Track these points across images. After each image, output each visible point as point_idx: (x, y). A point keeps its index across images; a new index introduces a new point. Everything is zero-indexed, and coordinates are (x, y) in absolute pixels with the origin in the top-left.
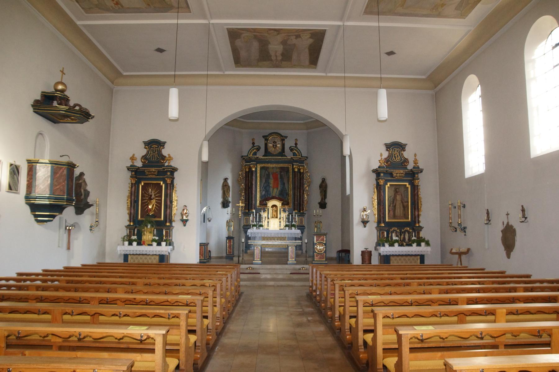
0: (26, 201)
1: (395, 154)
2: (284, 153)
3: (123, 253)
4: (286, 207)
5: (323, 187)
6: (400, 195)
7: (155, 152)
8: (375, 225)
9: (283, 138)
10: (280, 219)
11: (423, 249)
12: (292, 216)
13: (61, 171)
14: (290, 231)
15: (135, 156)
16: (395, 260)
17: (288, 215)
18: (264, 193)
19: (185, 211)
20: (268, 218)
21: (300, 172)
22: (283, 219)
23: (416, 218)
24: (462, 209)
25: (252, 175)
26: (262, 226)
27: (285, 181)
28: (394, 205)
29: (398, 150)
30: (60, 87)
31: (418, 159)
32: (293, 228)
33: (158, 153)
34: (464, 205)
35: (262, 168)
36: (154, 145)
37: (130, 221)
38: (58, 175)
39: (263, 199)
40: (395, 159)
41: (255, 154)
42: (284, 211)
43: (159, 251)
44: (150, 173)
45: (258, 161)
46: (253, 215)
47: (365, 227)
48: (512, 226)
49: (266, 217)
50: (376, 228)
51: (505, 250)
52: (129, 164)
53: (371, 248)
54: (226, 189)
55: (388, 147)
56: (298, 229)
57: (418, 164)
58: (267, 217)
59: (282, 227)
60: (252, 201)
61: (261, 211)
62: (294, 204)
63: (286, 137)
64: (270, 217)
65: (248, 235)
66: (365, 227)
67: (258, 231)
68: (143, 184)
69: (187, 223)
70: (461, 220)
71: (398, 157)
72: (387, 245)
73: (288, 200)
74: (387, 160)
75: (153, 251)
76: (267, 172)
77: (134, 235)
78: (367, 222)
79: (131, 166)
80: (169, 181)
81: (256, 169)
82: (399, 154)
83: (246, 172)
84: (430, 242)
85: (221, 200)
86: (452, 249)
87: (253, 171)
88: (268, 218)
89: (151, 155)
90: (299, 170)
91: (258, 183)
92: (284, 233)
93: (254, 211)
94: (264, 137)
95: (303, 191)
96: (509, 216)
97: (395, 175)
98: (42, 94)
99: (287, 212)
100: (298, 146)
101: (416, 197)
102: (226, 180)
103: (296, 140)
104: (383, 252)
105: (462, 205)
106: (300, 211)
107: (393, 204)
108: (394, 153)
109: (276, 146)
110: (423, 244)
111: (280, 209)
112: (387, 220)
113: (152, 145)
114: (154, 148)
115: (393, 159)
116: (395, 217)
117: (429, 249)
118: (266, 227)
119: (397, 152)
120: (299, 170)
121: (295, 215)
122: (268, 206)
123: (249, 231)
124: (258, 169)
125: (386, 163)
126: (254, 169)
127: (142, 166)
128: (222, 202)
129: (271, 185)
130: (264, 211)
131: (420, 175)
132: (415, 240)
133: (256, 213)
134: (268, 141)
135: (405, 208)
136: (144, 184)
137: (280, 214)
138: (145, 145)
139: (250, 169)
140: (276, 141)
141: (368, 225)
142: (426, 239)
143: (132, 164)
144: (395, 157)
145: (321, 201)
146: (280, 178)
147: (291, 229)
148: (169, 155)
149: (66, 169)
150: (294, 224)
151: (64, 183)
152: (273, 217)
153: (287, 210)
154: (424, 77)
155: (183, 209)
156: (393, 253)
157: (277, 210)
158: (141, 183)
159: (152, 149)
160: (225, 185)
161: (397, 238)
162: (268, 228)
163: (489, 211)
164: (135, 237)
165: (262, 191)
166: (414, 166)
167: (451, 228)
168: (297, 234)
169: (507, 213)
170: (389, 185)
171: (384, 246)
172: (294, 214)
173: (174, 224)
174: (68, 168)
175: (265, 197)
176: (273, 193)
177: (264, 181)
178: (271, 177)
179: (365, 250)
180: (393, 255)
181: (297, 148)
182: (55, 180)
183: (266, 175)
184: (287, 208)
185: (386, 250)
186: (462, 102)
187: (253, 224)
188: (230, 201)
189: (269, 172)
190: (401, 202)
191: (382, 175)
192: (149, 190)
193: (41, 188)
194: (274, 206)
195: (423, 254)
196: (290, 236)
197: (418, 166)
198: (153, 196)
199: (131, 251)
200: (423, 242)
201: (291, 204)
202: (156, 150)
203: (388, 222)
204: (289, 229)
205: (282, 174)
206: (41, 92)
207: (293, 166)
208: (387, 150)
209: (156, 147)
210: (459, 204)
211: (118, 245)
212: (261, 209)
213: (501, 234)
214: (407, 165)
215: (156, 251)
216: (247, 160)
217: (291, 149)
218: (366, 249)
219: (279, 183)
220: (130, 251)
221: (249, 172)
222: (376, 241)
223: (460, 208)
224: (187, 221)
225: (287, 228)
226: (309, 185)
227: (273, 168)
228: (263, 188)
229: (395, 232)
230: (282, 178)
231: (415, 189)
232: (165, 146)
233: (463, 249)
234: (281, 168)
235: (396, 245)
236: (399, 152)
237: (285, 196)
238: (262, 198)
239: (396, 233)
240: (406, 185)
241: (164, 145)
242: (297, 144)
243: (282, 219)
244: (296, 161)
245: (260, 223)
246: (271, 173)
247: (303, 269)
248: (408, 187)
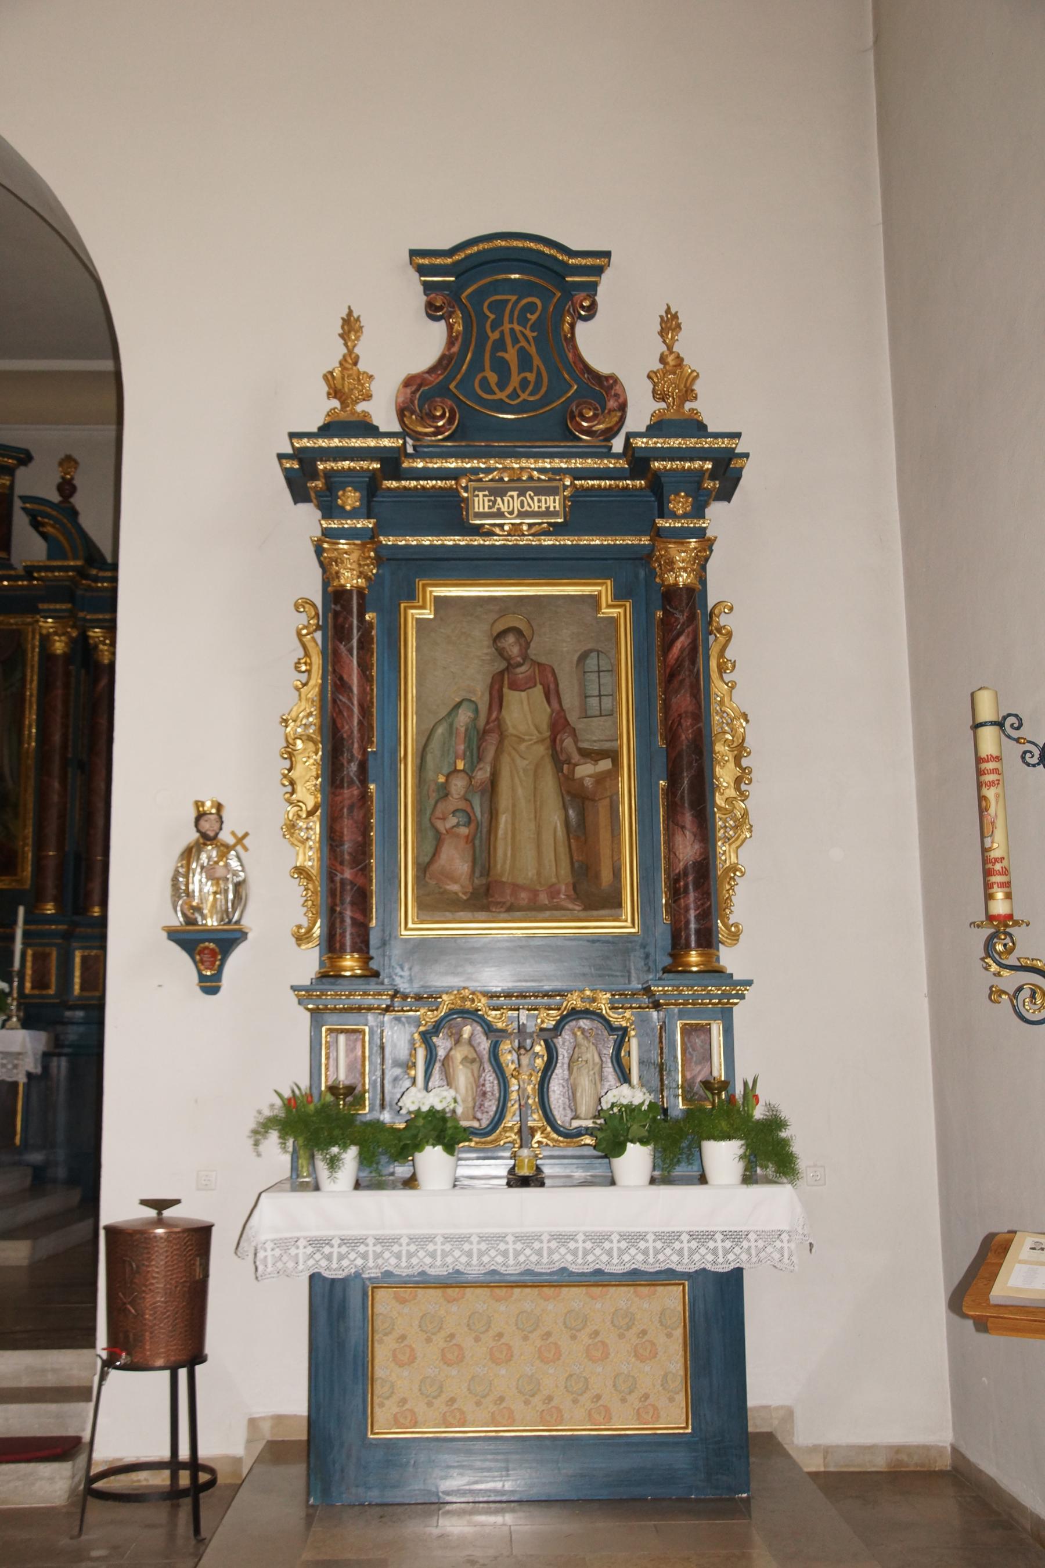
6: (538, 691)
28: (483, 774)
29: (531, 308)
108: (494, 336)
119: (523, 321)
144: (502, 368)
167: (1010, 980)
190: (541, 750)
195: (723, 1266)
218: (160, 1205)
240: (594, 601)
242: (73, 489)
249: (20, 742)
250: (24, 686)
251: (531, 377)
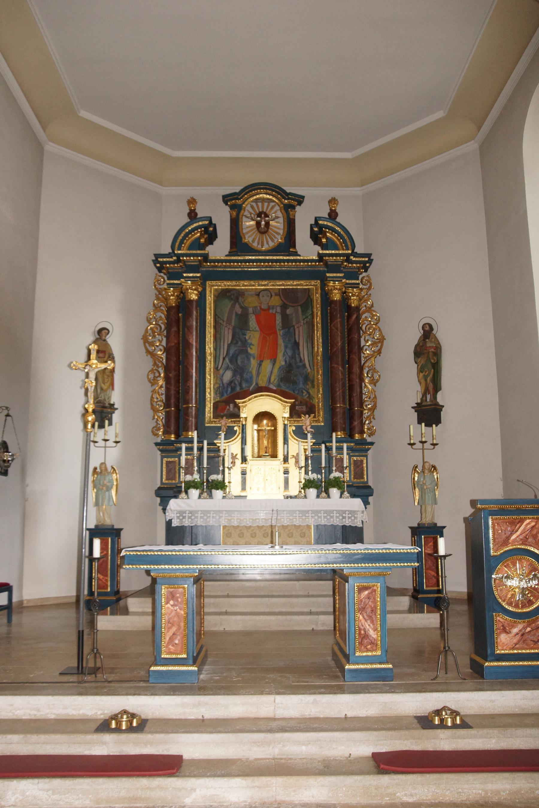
2: (294, 246)
4: (307, 421)
10: (286, 460)
12: (328, 449)
14: (324, 504)
17: (315, 450)
18: (228, 376)
20: (244, 460)
21: (349, 308)
22: (297, 462)
25: (188, 314)
32: (334, 492)
35: (221, 295)
39: (225, 396)
41: (197, 245)
42: (300, 433)
46: (189, 450)
49: (234, 457)
56: (353, 496)
58: (239, 456)
59: (295, 488)
60: (187, 401)
61: (217, 436)
62: (332, 412)
63: (300, 200)
64: (248, 453)
67: (206, 504)
76: (237, 306)
81: (202, 296)
83: (169, 309)
87: (191, 301)
88: (244, 460)
91: (210, 348)
92: (304, 513)
93: (195, 434)
94: (226, 199)
95: (361, 368)
99: (309, 436)
106: (351, 436)
109: (267, 224)
111: (285, 426)
118: (234, 488)
120: (345, 298)
121: (340, 449)
122: (243, 415)
123: (173, 503)
124: (210, 299)
126: (194, 297)
129: (253, 350)
130: (230, 434)
133: (200, 442)
134: (242, 211)
139: (182, 294)
145: (422, 399)
146: (283, 327)
147: (329, 497)
150: (336, 478)
152: (259, 457)
153: (309, 429)
157: (276, 429)
162: (243, 494)
165: (221, 371)
168: (351, 512)
172: (334, 444)
175: (233, 389)
176: (258, 374)
177: (228, 336)
178: (253, 322)
183: (234, 316)
184: (308, 423)
187: (189, 478)
189: (245, 309)
194: (260, 417)
196: (323, 522)
204: (318, 496)
205: (288, 311)
207: (323, 285)
212: (219, 429)
217: (316, 238)
219: (280, 341)
225: (312, 492)
226: (379, 352)
227: (258, 294)
228: (227, 360)
234: (285, 293)
237: (301, 385)
238: (222, 395)
243: (292, 461)
244: (336, 268)
245: (213, 477)
246: (251, 310)
249: (313, 348)
250: (313, 318)
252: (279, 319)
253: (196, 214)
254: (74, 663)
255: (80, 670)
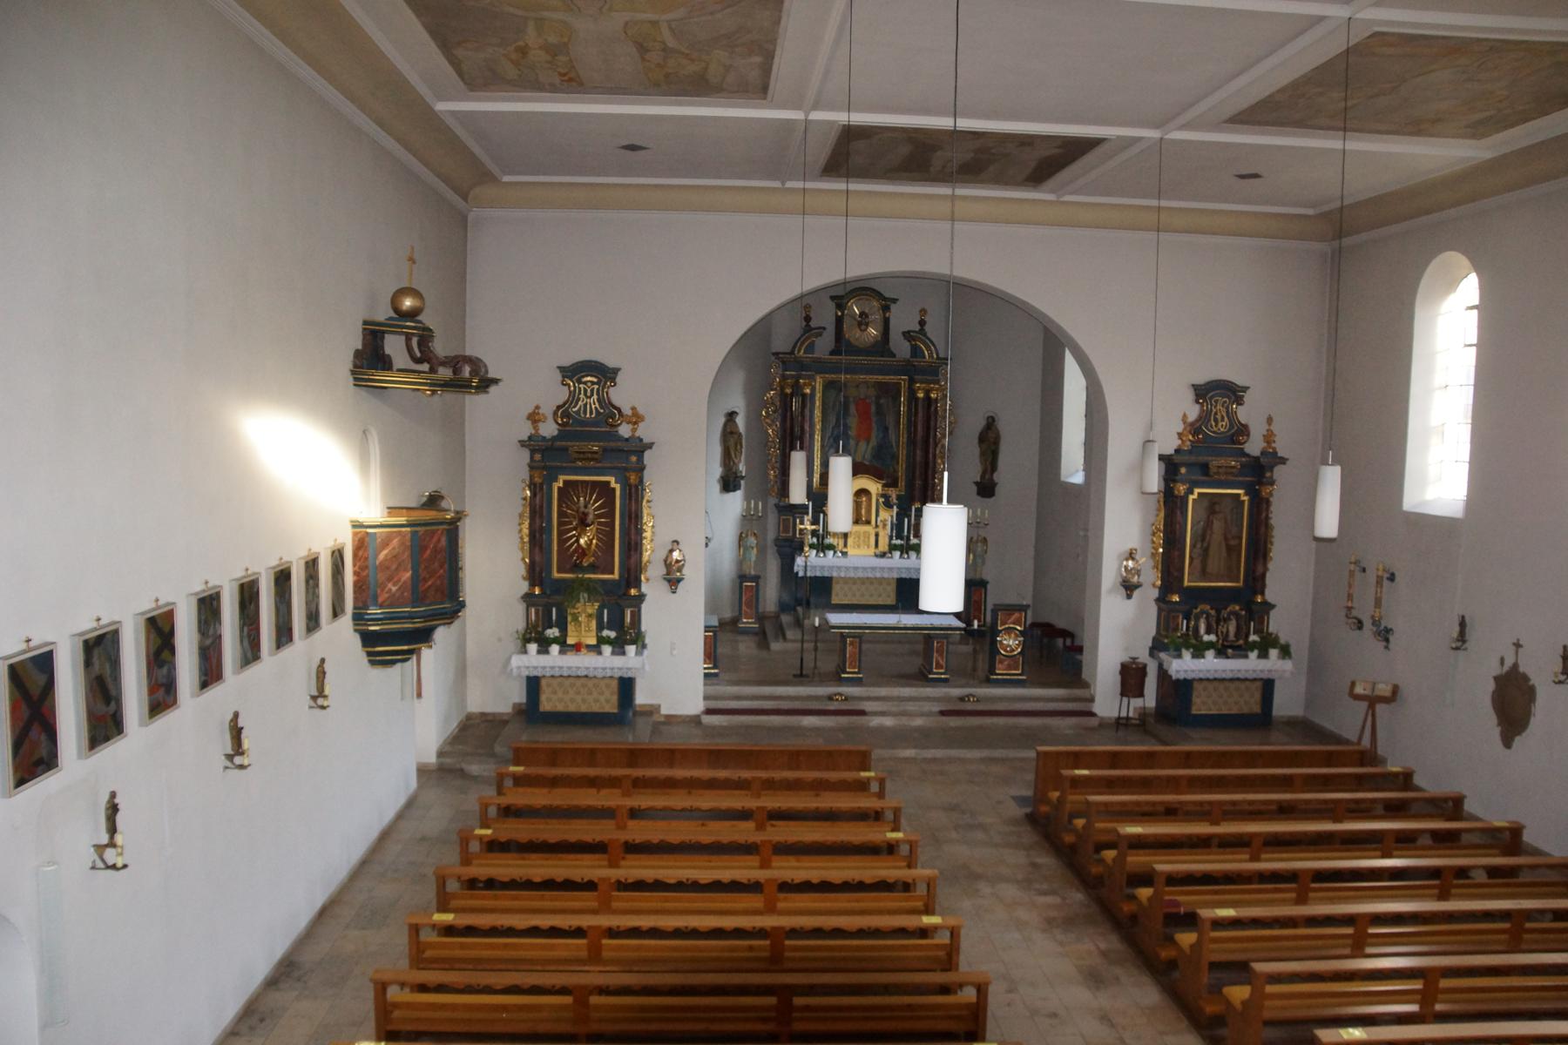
0: (355, 625)
1: (1216, 414)
3: (526, 673)
4: (893, 494)
5: (989, 440)
7: (592, 395)
8: (1155, 593)
9: (886, 304)
11: (1273, 664)
13: (435, 539)
15: (541, 411)
16: (1205, 689)
19: (676, 555)
23: (1256, 582)
24: (1386, 583)
26: (831, 547)
27: (890, 421)
28: (1205, 545)
29: (1225, 402)
30: (408, 303)
31: (1275, 432)
33: (598, 400)
34: (1393, 574)
35: (828, 386)
36: (587, 376)
37: (532, 585)
38: (428, 552)
40: (1216, 426)
42: (888, 505)
43: (620, 669)
44: (582, 456)
45: (820, 367)
47: (1129, 597)
48: (1525, 678)
50: (1158, 600)
51: (1499, 724)
52: (526, 430)
53: (1143, 656)
54: (731, 443)
55: (1203, 392)
57: (1273, 445)
63: (895, 301)
65: (797, 573)
66: (1129, 597)
68: (561, 485)
69: (681, 585)
70: (1380, 613)
71: (1223, 420)
72: (1187, 655)
73: (896, 471)
74: (1195, 428)
75: (604, 669)
77: (551, 627)
78: (1138, 586)
79: (530, 438)
80: (633, 478)
81: (813, 389)
82: (1227, 412)
84: (1292, 650)
85: (718, 471)
86: (1353, 684)
89: (580, 403)
90: (927, 392)
92: (891, 569)
96: (1520, 650)
97: (1213, 470)
98: (364, 329)
99: (895, 507)
100: (927, 328)
101: (1263, 529)
102: (731, 416)
103: (923, 311)
104: (1178, 672)
105: (1386, 575)
107: (1203, 540)
108: (1214, 410)
110: (1274, 653)
111: (877, 500)
112: (1186, 583)
113: (583, 377)
114: (589, 384)
115: (1211, 427)
116: (1204, 574)
117: (1287, 665)
119: (1223, 406)
120: (927, 392)
125: (1193, 436)
126: (808, 391)
127: (556, 433)
128: (722, 477)
131: (1279, 472)
132: (1254, 642)
135: (1232, 550)
136: (565, 482)
137: (877, 515)
138: (564, 377)
140: (867, 311)
141: (1136, 593)
142: (1282, 641)
143: (533, 432)
147: (908, 557)
148: (633, 409)
149: (445, 532)
151: (442, 571)
153: (895, 501)
154: (1310, 212)
155: (670, 548)
156: (1202, 676)
158: (556, 480)
159: (581, 386)
160: (732, 433)
161: (1212, 638)
162: (845, 550)
163: (1467, 620)
164: (553, 632)
165: (827, 449)
166: (1264, 448)
167: (1350, 621)
169: (1515, 641)
170: (1195, 496)
171: (1179, 656)
173: (644, 588)
174: (448, 530)
177: (832, 419)
179: (1128, 660)
180: (1201, 680)
181: (925, 335)
182: (423, 566)
185: (1185, 668)
186: (1417, 310)
188: (744, 474)
191: (1183, 470)
192: (579, 500)
193: (390, 590)
196: (904, 576)
197: (1274, 449)
198: (591, 517)
199: (548, 669)
200: (1274, 648)
201: (902, 483)
202: (592, 390)
203: (1188, 588)
204: (901, 556)
205: (882, 401)
206: (361, 322)
208: (1197, 402)
209: (593, 383)
210: (1380, 573)
211: (513, 653)
213: (1491, 686)
214: (1245, 443)
215: (612, 669)
216: (786, 360)
218: (1134, 659)
219: (874, 425)
220: (544, 668)
221: (792, 395)
222: (1153, 632)
223: (1382, 580)
224: (679, 580)
228: (832, 440)
229: (1204, 616)
230: (880, 412)
231: (1260, 506)
232: (618, 380)
233: (1384, 689)
234: (880, 385)
235: (1210, 654)
236: (1227, 408)
239: (1207, 618)
240: (1239, 495)
241: (615, 379)
246: (851, 399)
247: (972, 699)
248: (1244, 501)
251: (1224, 424)
252: (873, 408)
253: (810, 319)
254: (799, 672)
255: (801, 675)
